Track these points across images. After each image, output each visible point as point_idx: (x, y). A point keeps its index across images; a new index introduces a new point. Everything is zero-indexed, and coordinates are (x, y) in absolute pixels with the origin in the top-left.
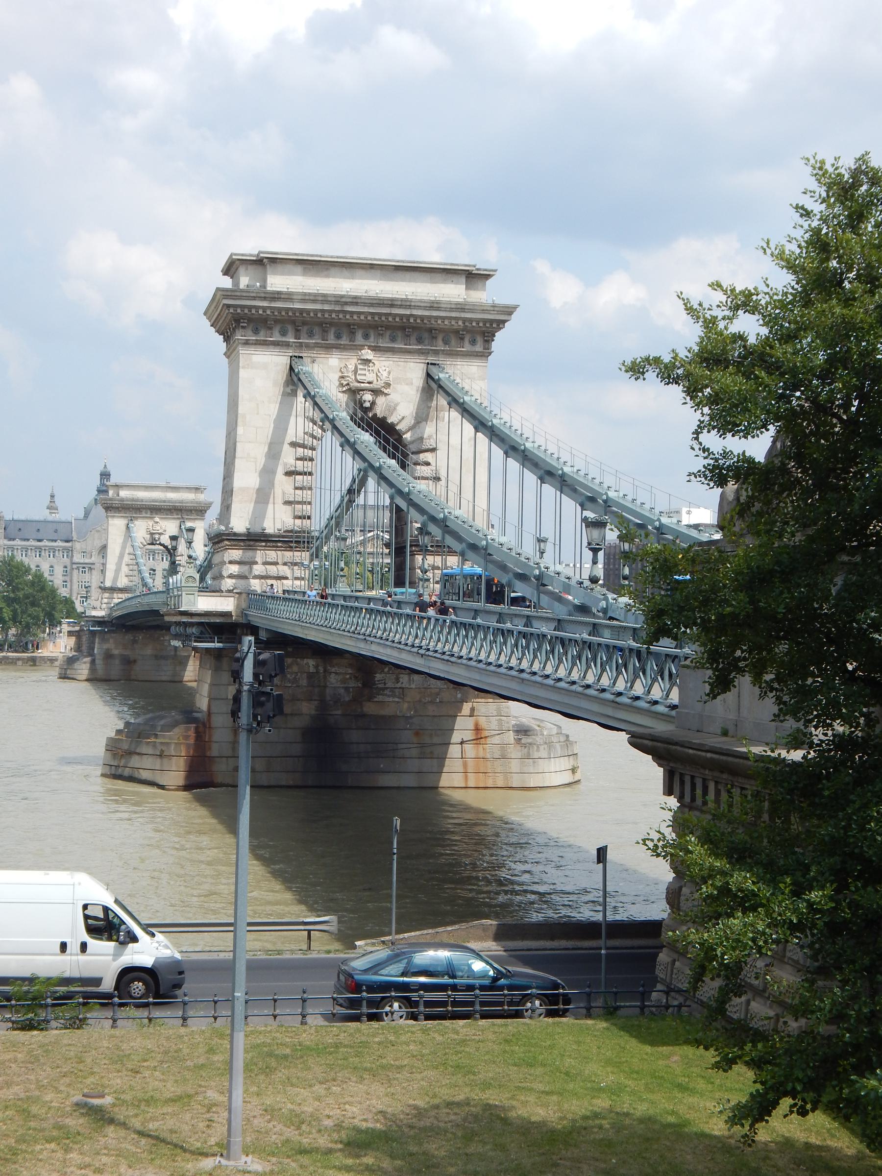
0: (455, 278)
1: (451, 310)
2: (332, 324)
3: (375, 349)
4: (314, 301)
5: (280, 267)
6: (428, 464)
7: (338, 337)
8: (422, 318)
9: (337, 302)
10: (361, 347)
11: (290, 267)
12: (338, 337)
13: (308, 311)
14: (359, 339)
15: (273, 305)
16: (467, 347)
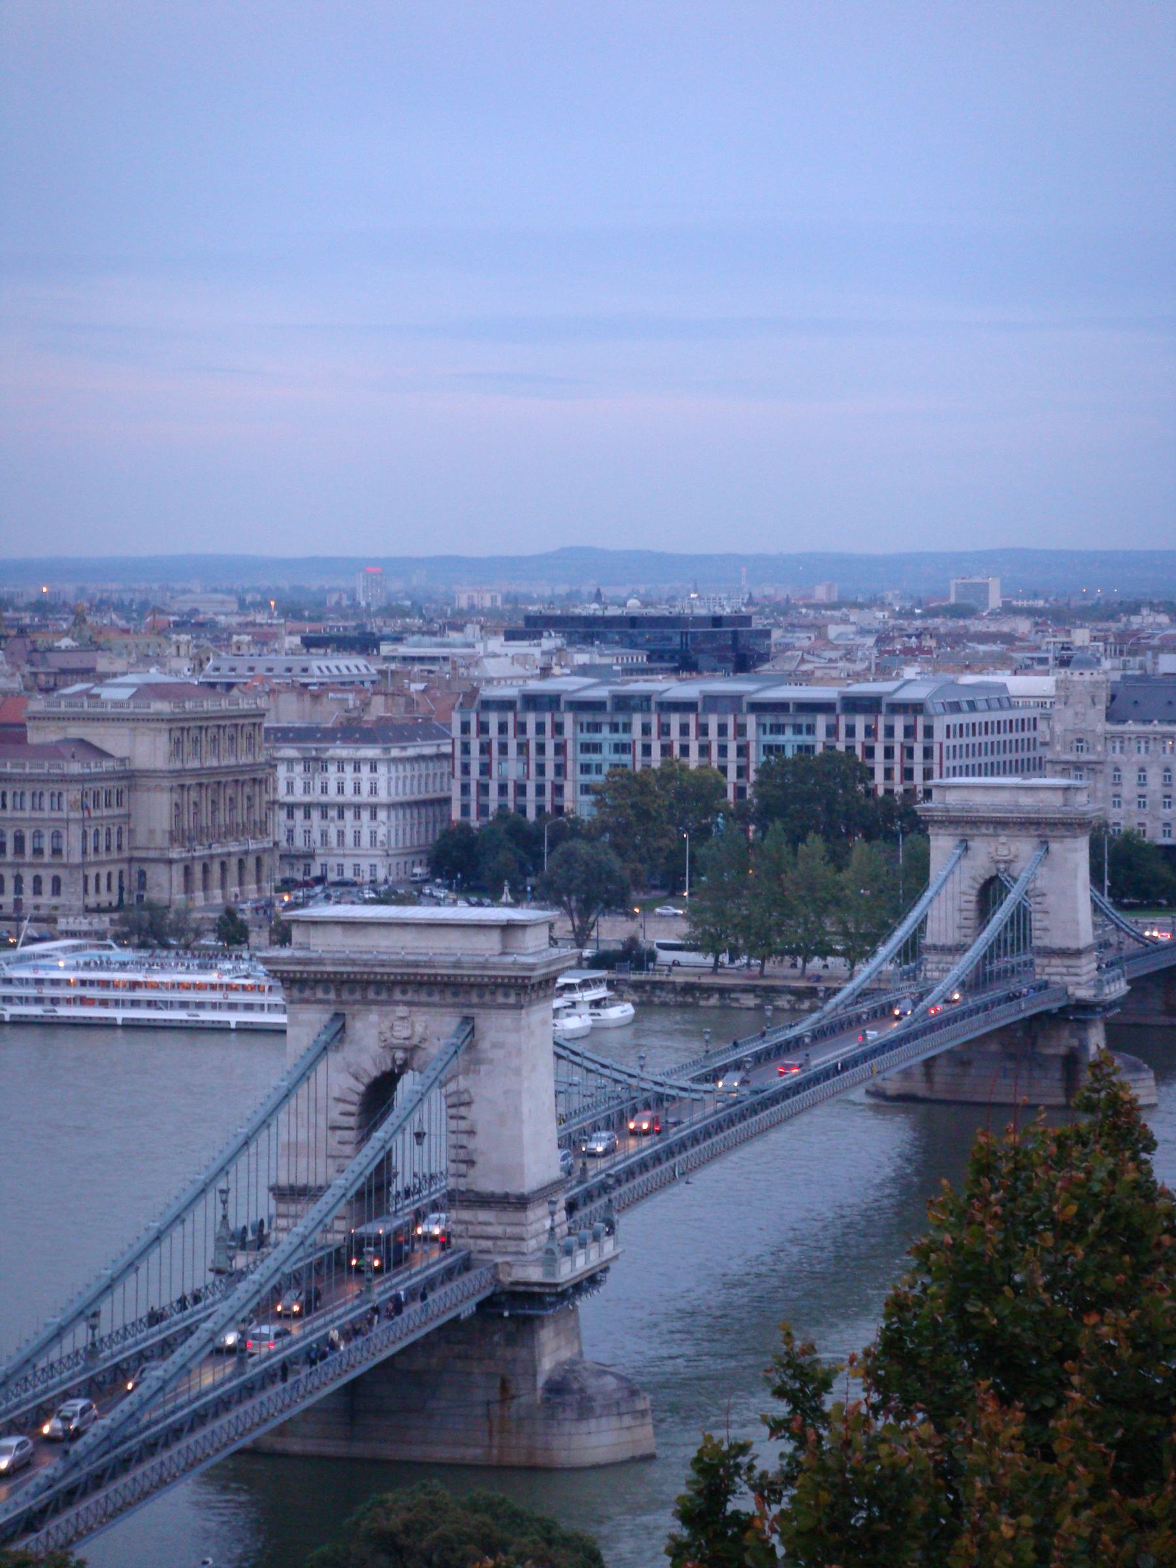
0: (486, 931)
1: (474, 968)
2: (369, 983)
3: (409, 1004)
4: (345, 964)
5: (320, 928)
6: (463, 1118)
7: (378, 993)
8: (449, 976)
9: (365, 965)
10: (397, 1003)
11: (329, 928)
12: (378, 993)
13: (342, 973)
14: (398, 996)
15: (308, 968)
16: (501, 999)
